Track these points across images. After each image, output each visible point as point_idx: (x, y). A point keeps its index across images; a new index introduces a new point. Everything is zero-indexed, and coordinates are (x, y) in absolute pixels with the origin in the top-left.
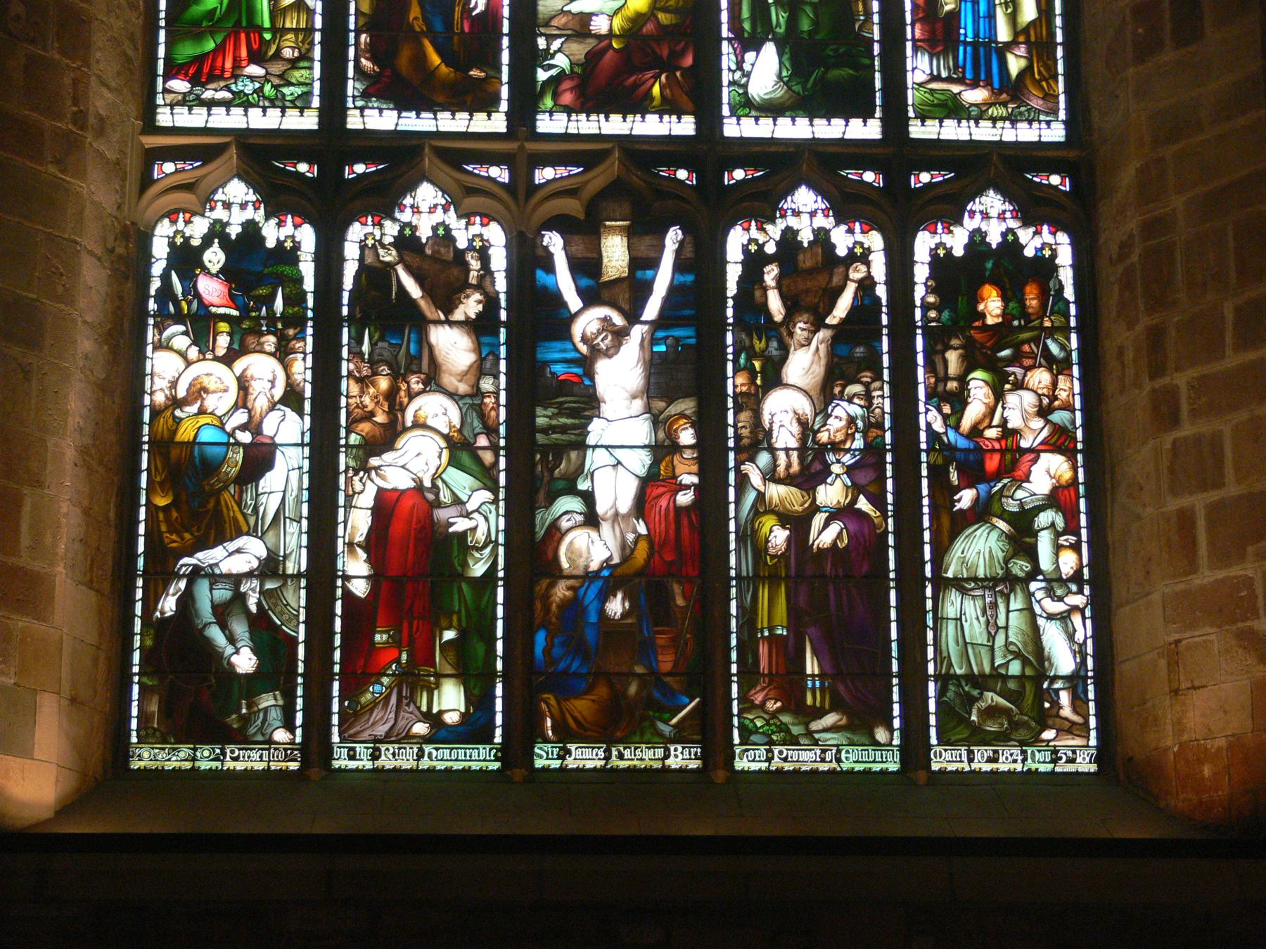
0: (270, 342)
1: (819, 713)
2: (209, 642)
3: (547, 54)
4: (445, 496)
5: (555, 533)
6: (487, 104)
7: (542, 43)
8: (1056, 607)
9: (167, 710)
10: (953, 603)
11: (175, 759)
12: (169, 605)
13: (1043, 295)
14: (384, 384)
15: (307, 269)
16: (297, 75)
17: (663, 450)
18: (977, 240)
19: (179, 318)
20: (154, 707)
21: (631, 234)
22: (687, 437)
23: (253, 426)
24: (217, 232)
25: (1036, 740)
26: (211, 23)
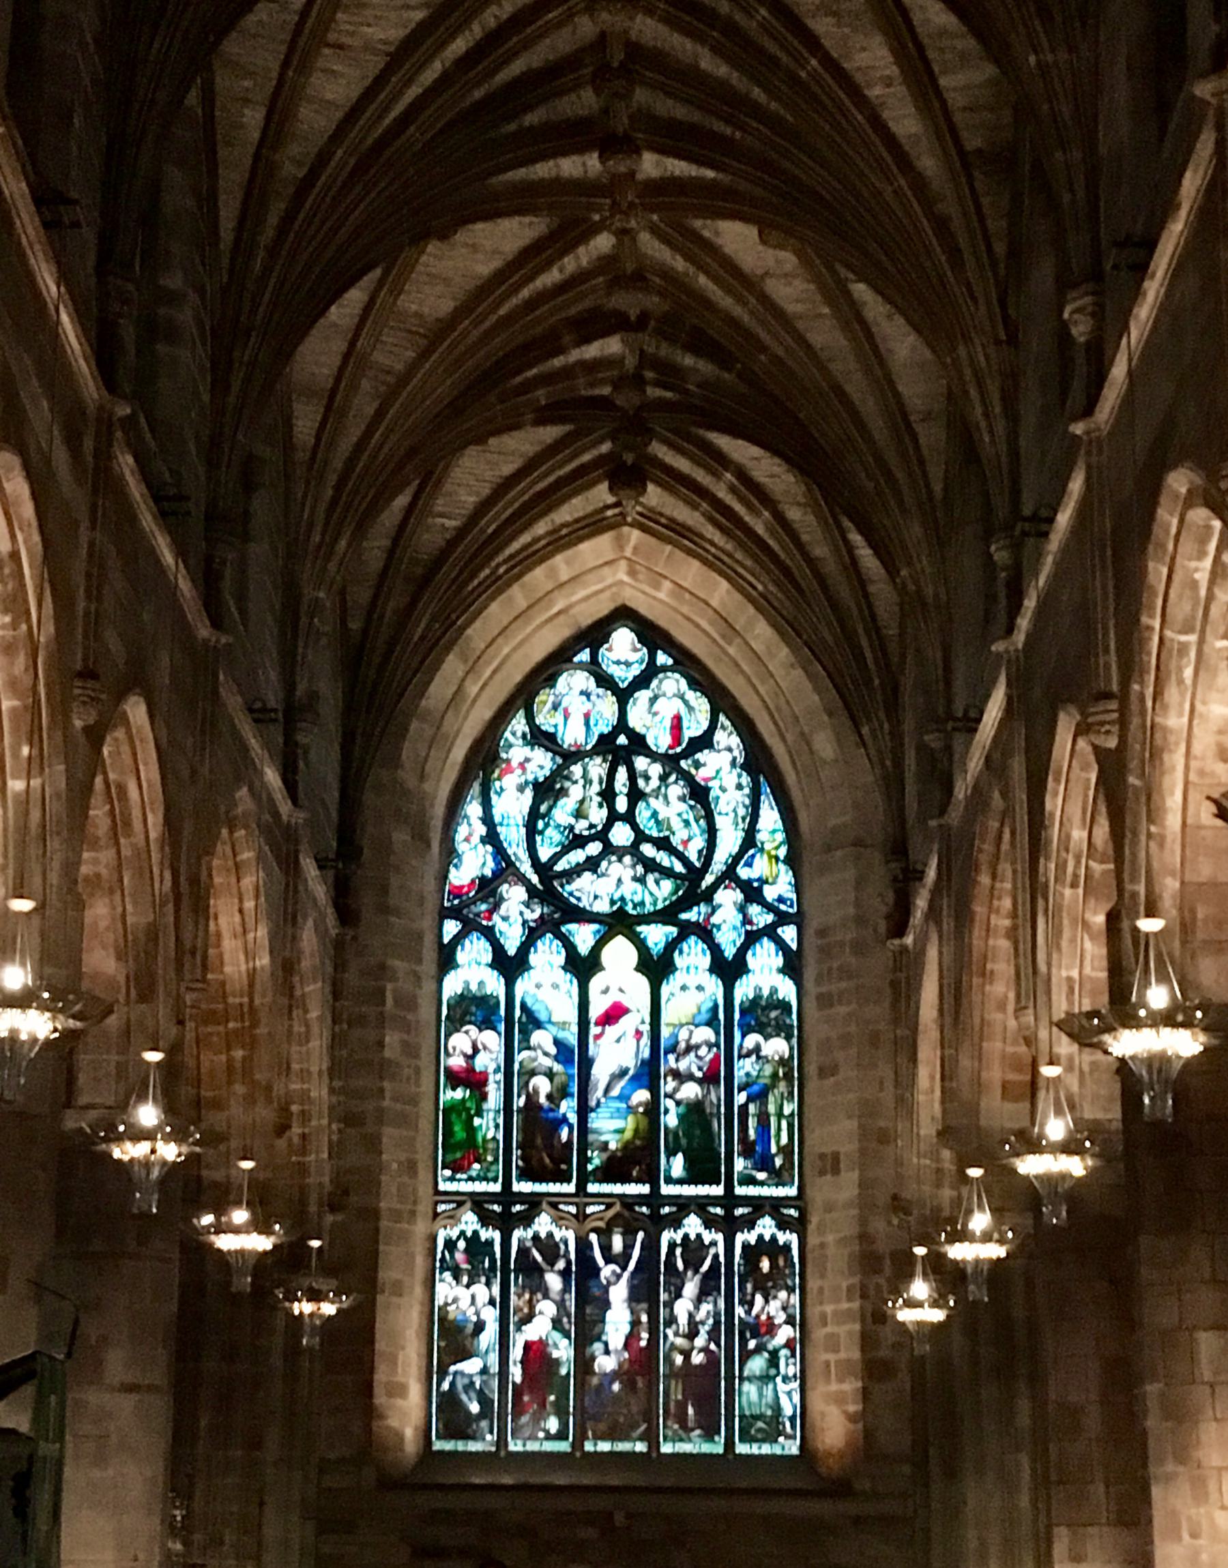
0: (483, 1279)
1: (693, 1430)
2: (461, 1401)
3: (591, 1158)
4: (550, 1342)
5: (593, 1358)
6: (569, 1181)
7: (589, 1153)
8: (787, 1388)
9: (446, 1426)
10: (747, 1387)
11: (448, 1446)
12: (446, 1386)
13: (786, 1261)
14: (527, 1296)
15: (497, 1248)
16: (494, 1168)
17: (635, 1323)
18: (761, 1237)
19: (448, 1269)
20: (441, 1426)
21: (624, 1234)
22: (644, 1318)
23: (477, 1313)
24: (463, 1233)
25: (776, 1441)
26: (458, 1146)
